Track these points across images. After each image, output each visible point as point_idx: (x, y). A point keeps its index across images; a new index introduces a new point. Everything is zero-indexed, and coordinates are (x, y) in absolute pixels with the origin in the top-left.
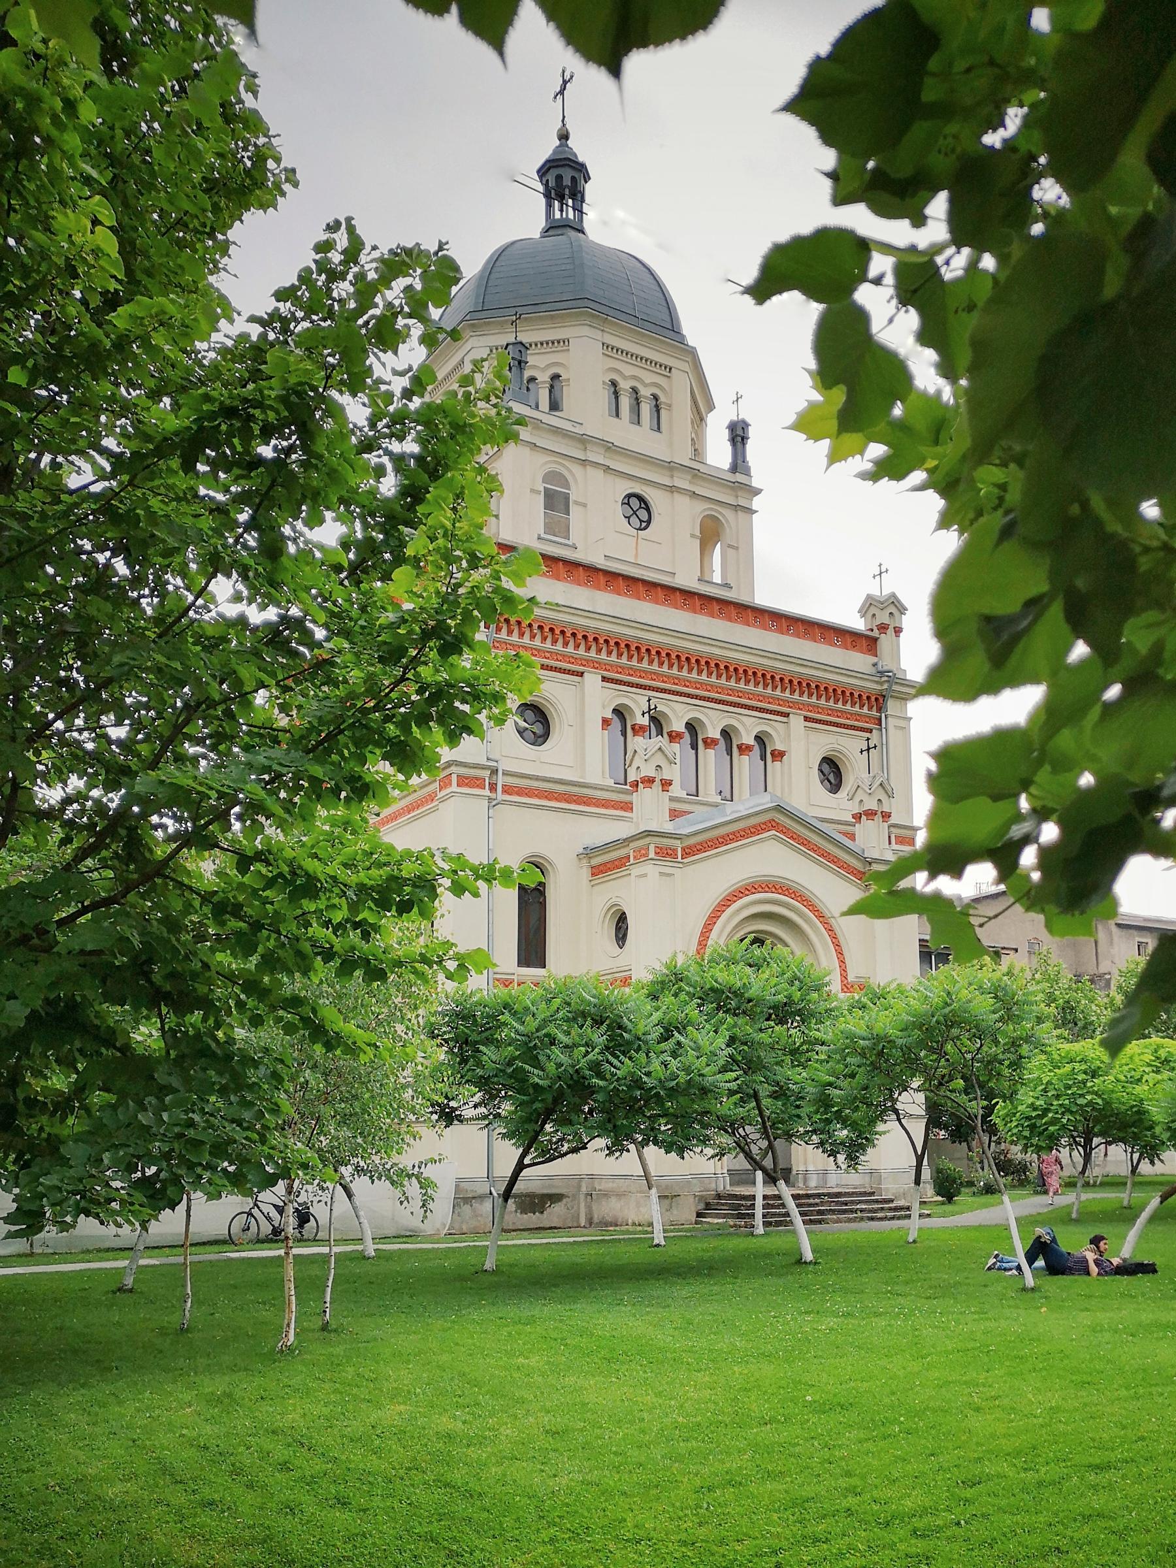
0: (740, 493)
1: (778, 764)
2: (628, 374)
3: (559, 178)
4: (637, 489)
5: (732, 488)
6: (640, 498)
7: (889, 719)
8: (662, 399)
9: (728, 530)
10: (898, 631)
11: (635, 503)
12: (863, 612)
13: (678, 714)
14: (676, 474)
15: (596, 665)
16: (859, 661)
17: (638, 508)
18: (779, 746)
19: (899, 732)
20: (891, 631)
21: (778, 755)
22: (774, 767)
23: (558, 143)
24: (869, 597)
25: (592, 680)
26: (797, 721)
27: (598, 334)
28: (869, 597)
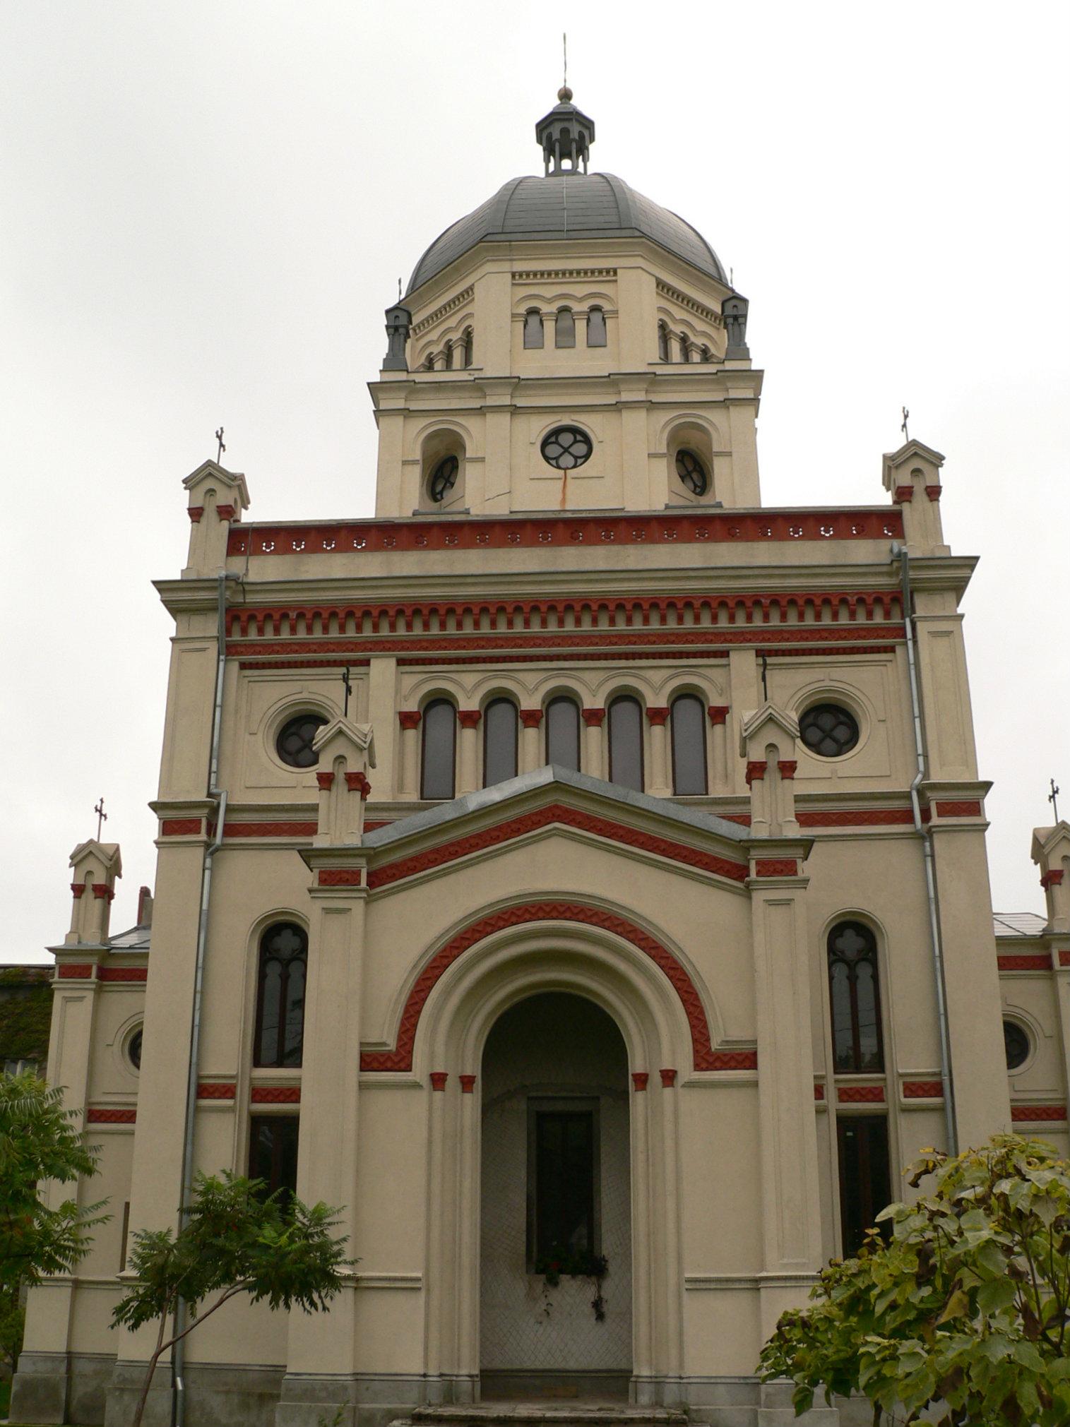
0: (729, 385)
1: (718, 728)
2: (548, 296)
3: (565, 132)
4: (566, 420)
5: (717, 382)
6: (574, 431)
7: (919, 625)
8: (607, 306)
9: (714, 435)
10: (934, 492)
11: (566, 439)
12: (887, 482)
13: (531, 688)
14: (622, 387)
15: (383, 646)
16: (865, 551)
17: (567, 445)
18: (715, 701)
19: (943, 643)
20: (920, 496)
21: (720, 715)
22: (716, 734)
23: (558, 102)
24: (886, 458)
25: (383, 669)
26: (744, 662)
27: (506, 266)
28: (885, 457)
